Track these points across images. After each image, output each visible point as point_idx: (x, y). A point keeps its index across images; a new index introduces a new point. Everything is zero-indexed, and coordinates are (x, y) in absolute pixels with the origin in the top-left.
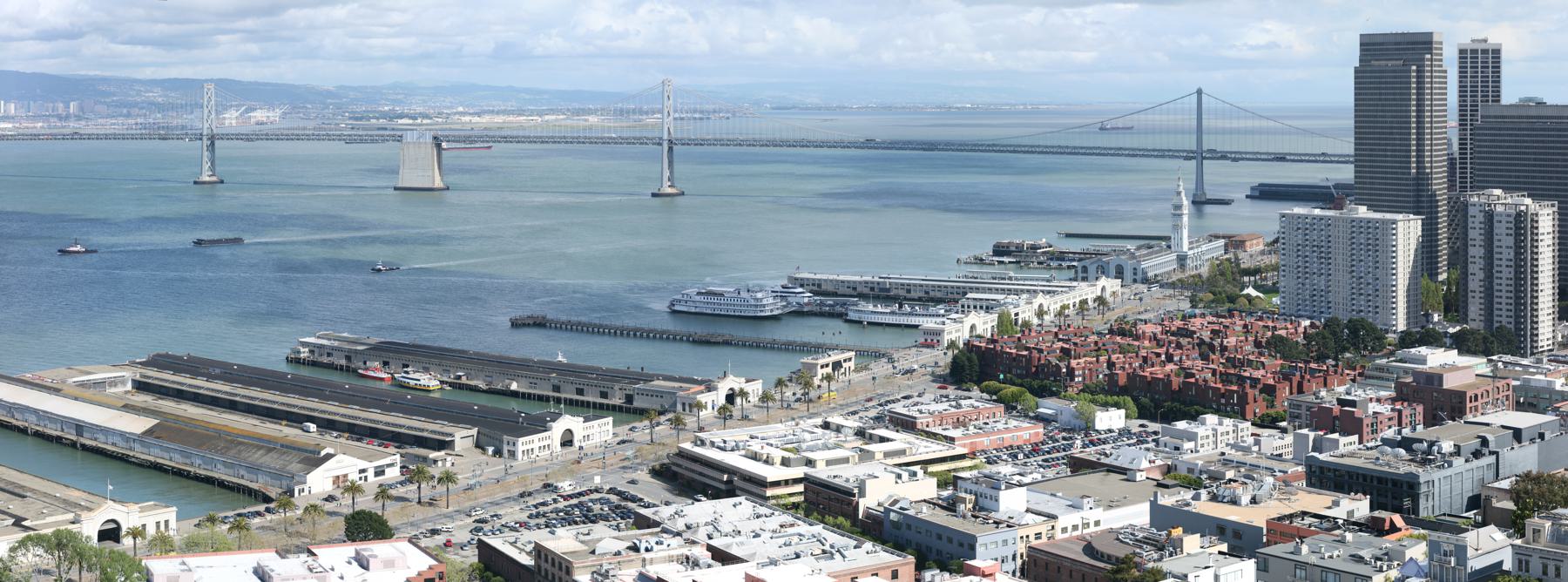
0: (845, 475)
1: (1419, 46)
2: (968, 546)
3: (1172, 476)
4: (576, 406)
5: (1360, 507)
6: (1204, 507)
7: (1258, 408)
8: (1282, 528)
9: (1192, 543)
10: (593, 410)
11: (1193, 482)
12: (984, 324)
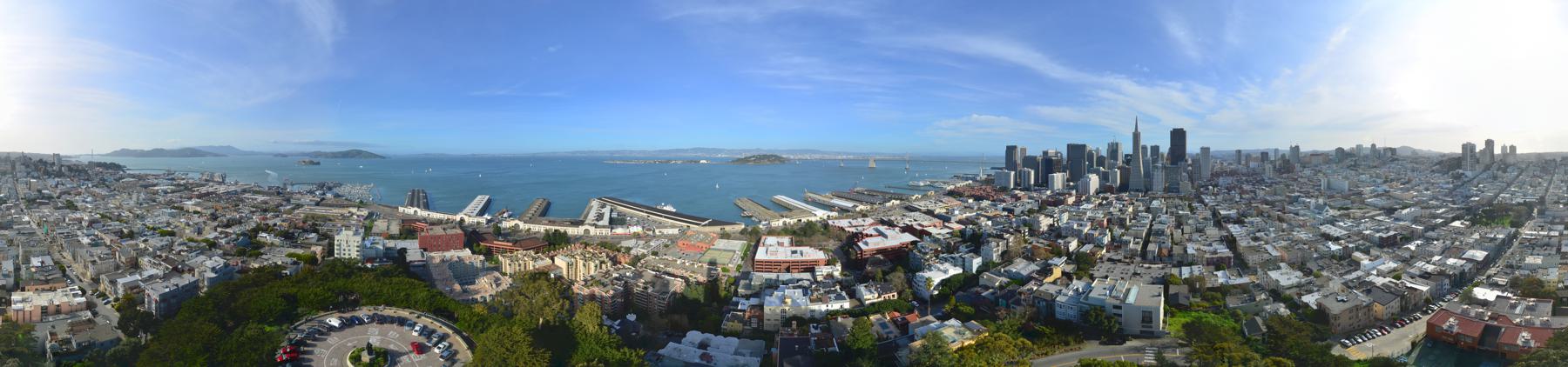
0: (932, 209)
1: (1014, 148)
2: (950, 219)
3: (979, 209)
4: (894, 199)
5: (1006, 213)
6: (983, 213)
7: (991, 199)
8: (995, 216)
9: (982, 218)
10: (897, 199)
11: (982, 210)
12: (953, 187)
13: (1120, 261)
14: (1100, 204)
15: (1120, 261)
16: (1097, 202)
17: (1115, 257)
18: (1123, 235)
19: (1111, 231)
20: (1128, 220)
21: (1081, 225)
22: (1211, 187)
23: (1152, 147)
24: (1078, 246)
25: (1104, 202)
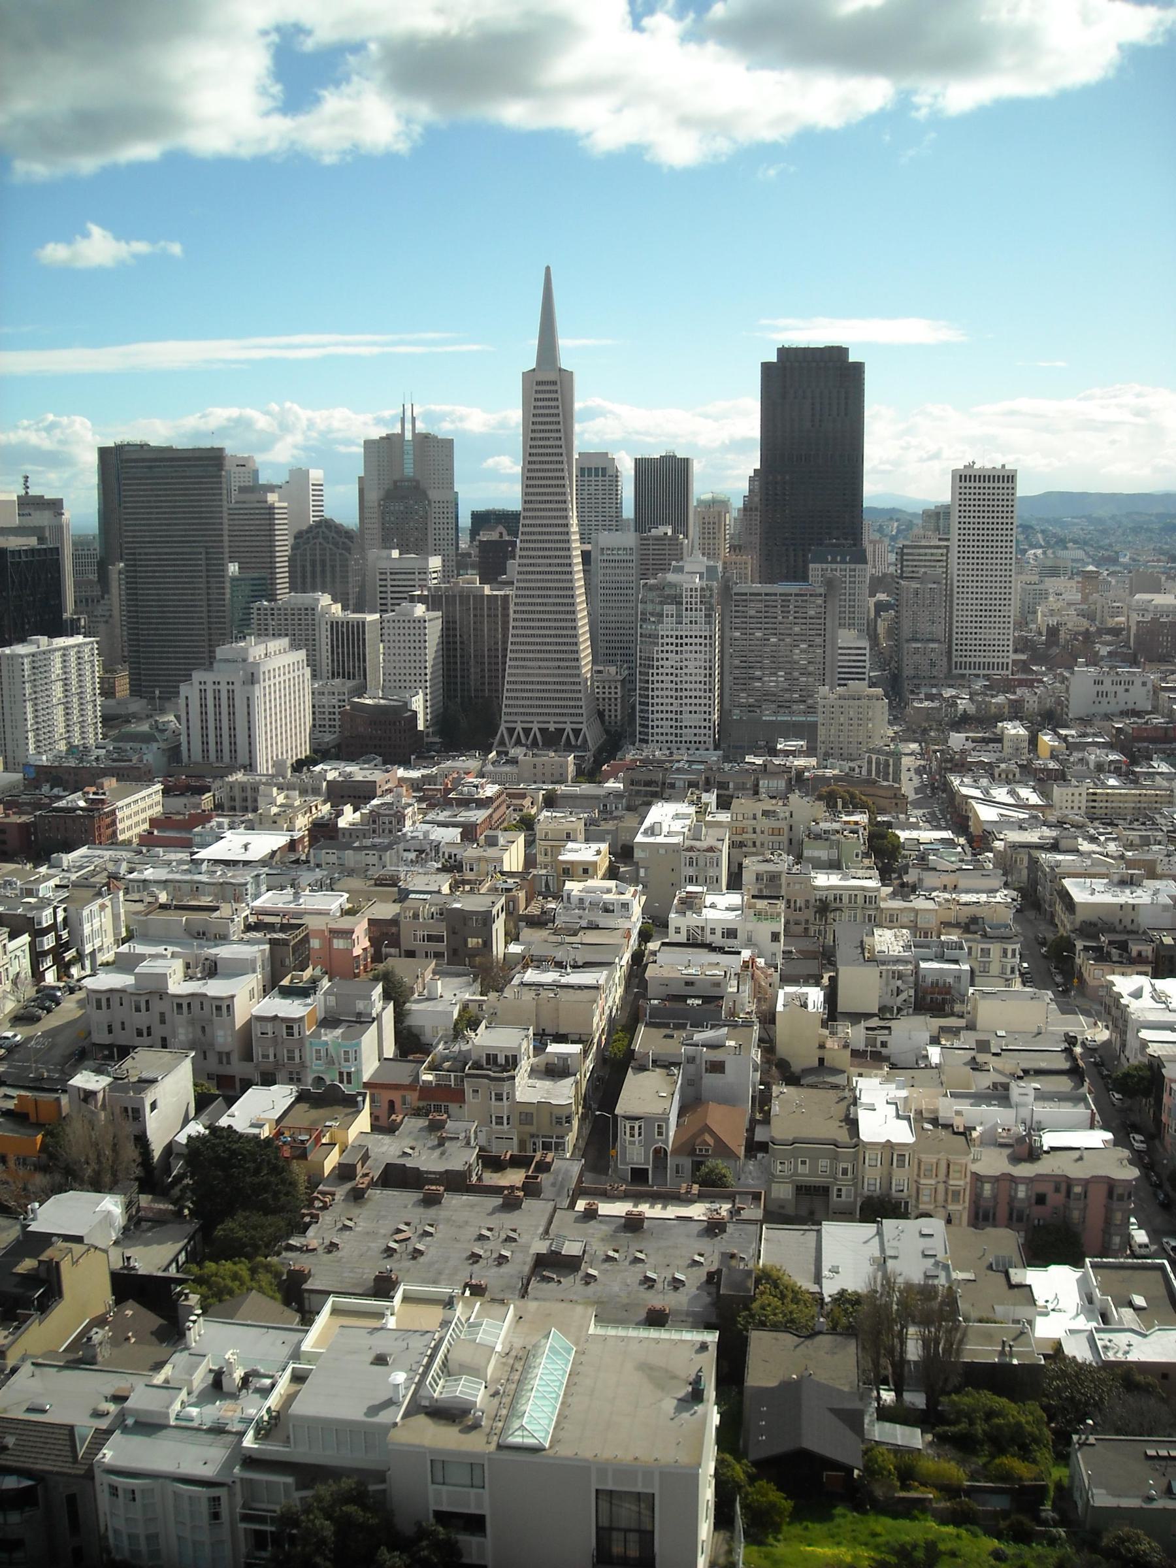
13: (457, 1182)
14: (323, 832)
15: (457, 1182)
16: (302, 822)
17: (427, 1161)
18: (469, 1020)
19: (396, 994)
20: (499, 926)
21: (212, 970)
22: (1014, 730)
23: (642, 466)
24: (202, 1102)
25: (349, 817)
